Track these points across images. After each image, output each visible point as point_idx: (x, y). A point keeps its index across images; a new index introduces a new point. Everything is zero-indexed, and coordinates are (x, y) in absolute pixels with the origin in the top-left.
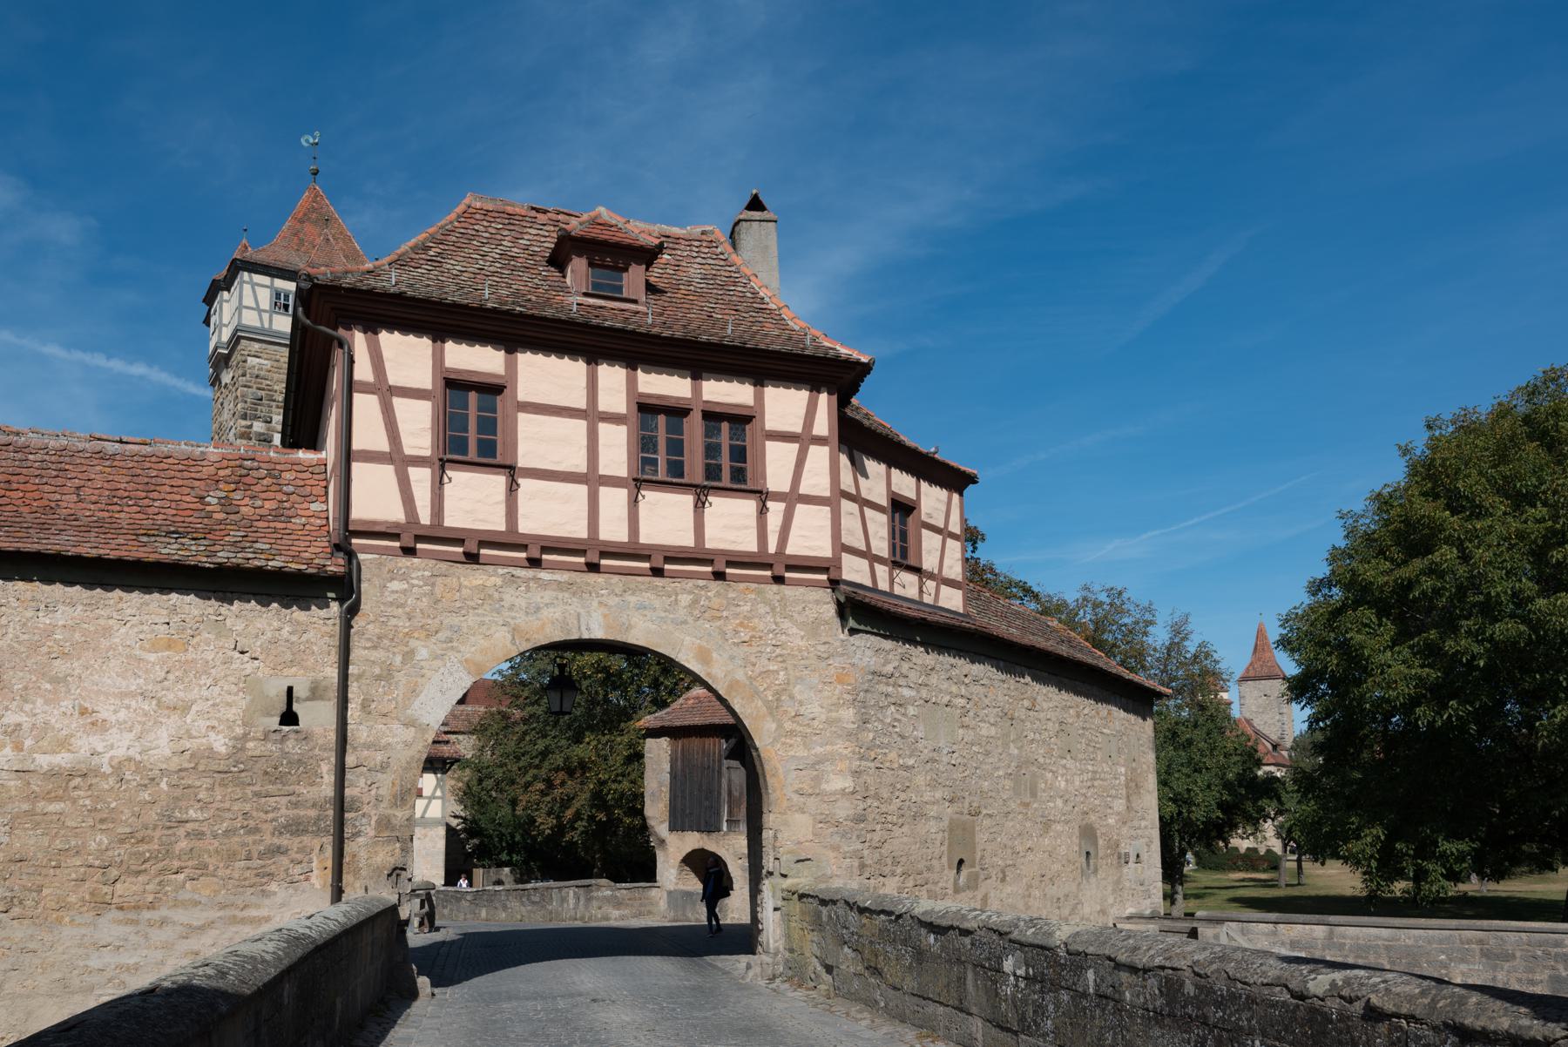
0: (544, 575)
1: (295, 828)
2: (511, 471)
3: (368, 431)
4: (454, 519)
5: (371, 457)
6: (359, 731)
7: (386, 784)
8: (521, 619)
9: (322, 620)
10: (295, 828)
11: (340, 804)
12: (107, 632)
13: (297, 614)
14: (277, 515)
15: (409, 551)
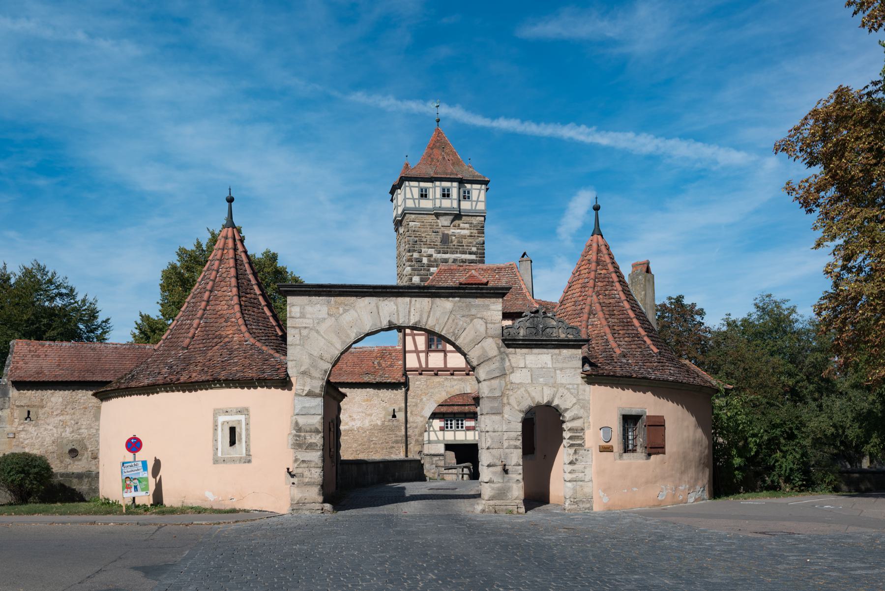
0: (455, 377)
1: (397, 442)
2: (445, 352)
3: (410, 346)
4: (431, 365)
5: (411, 352)
6: (410, 419)
7: (417, 431)
8: (449, 389)
9: (400, 393)
10: (397, 442)
11: (406, 436)
12: (354, 398)
13: (395, 391)
14: (391, 366)
15: (421, 374)
